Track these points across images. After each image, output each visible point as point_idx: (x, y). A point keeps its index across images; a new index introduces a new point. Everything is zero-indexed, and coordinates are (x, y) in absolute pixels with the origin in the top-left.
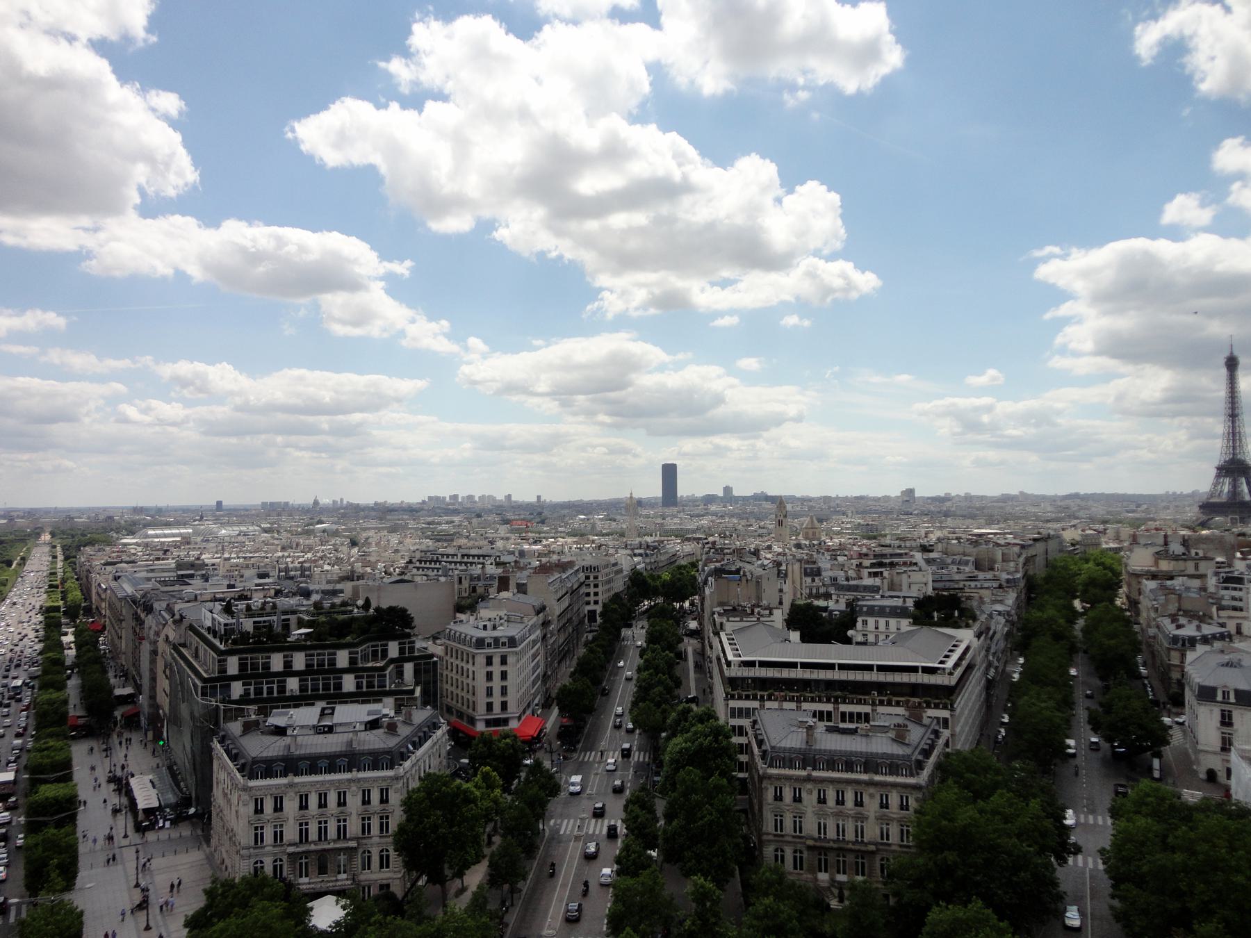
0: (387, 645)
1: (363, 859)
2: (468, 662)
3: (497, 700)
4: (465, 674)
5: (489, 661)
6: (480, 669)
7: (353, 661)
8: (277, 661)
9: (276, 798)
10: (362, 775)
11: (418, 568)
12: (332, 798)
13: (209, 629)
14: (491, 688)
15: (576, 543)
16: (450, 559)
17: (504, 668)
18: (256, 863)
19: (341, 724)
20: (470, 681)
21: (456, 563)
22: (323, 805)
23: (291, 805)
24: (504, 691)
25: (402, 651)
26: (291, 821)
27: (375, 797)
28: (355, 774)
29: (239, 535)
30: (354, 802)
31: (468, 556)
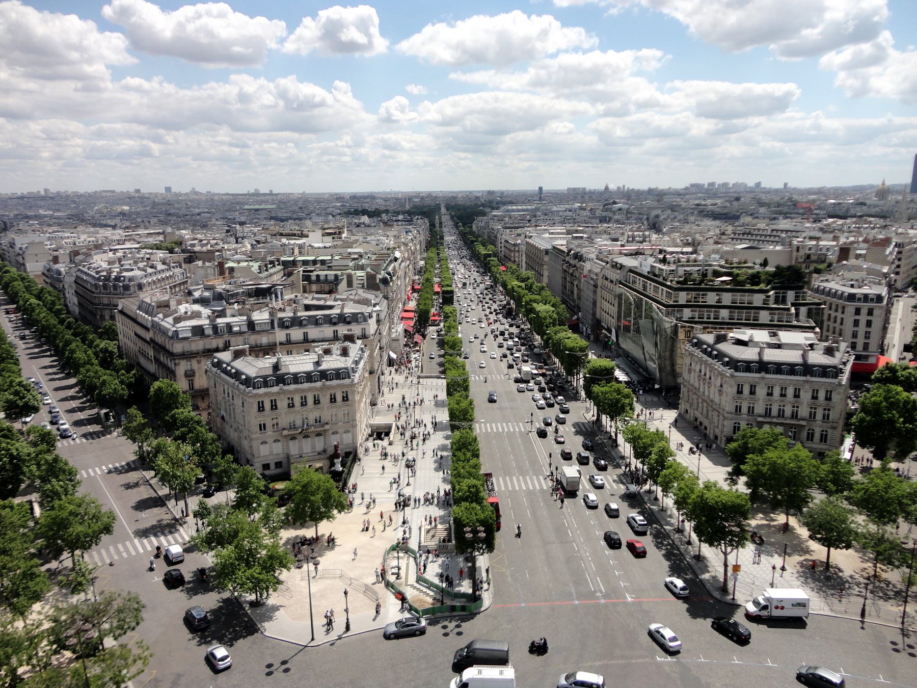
0: (786, 293)
1: (808, 434)
2: (836, 311)
3: (860, 341)
4: (832, 319)
5: (858, 311)
6: (849, 317)
7: (765, 302)
8: (711, 298)
9: (751, 386)
10: (813, 379)
11: (733, 239)
12: (790, 392)
13: (648, 272)
14: (857, 331)
15: (854, 223)
16: (761, 232)
17: (870, 318)
18: (735, 423)
19: (788, 344)
20: (837, 325)
21: (766, 236)
22: (783, 395)
23: (761, 392)
24: (867, 335)
25: (797, 297)
26: (761, 402)
27: (822, 395)
28: (809, 378)
29: (565, 211)
30: (806, 396)
31: (777, 231)
